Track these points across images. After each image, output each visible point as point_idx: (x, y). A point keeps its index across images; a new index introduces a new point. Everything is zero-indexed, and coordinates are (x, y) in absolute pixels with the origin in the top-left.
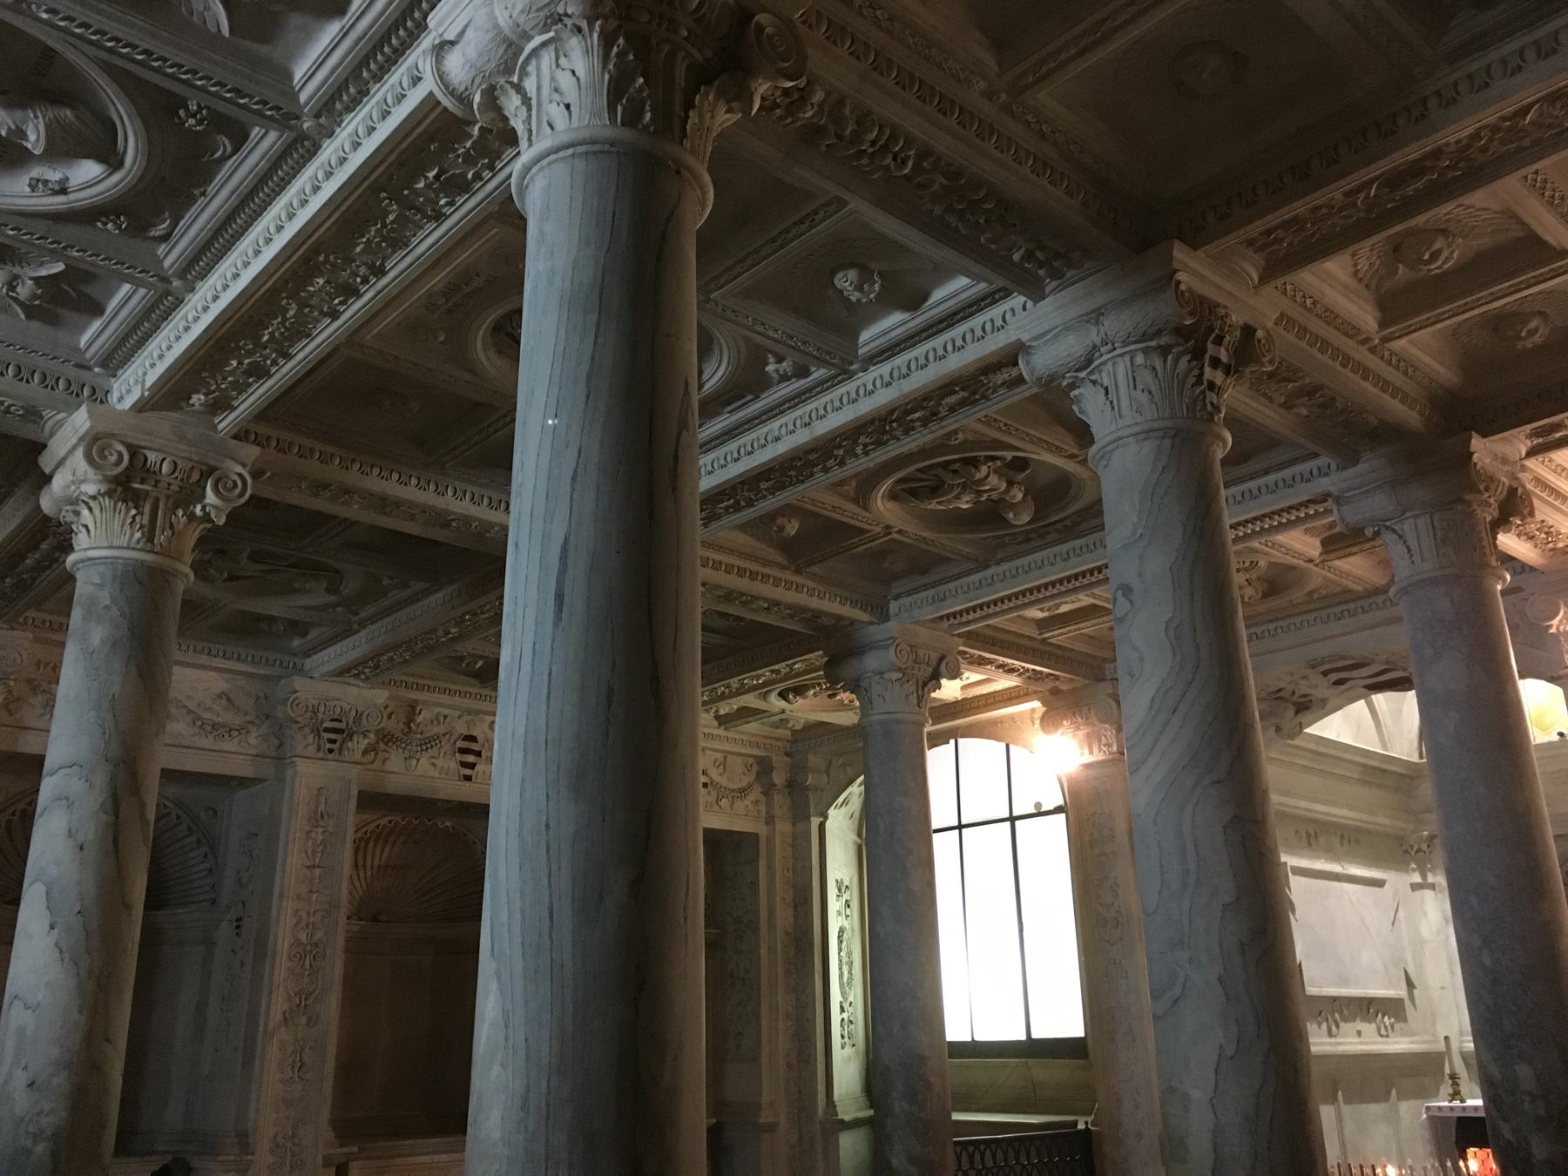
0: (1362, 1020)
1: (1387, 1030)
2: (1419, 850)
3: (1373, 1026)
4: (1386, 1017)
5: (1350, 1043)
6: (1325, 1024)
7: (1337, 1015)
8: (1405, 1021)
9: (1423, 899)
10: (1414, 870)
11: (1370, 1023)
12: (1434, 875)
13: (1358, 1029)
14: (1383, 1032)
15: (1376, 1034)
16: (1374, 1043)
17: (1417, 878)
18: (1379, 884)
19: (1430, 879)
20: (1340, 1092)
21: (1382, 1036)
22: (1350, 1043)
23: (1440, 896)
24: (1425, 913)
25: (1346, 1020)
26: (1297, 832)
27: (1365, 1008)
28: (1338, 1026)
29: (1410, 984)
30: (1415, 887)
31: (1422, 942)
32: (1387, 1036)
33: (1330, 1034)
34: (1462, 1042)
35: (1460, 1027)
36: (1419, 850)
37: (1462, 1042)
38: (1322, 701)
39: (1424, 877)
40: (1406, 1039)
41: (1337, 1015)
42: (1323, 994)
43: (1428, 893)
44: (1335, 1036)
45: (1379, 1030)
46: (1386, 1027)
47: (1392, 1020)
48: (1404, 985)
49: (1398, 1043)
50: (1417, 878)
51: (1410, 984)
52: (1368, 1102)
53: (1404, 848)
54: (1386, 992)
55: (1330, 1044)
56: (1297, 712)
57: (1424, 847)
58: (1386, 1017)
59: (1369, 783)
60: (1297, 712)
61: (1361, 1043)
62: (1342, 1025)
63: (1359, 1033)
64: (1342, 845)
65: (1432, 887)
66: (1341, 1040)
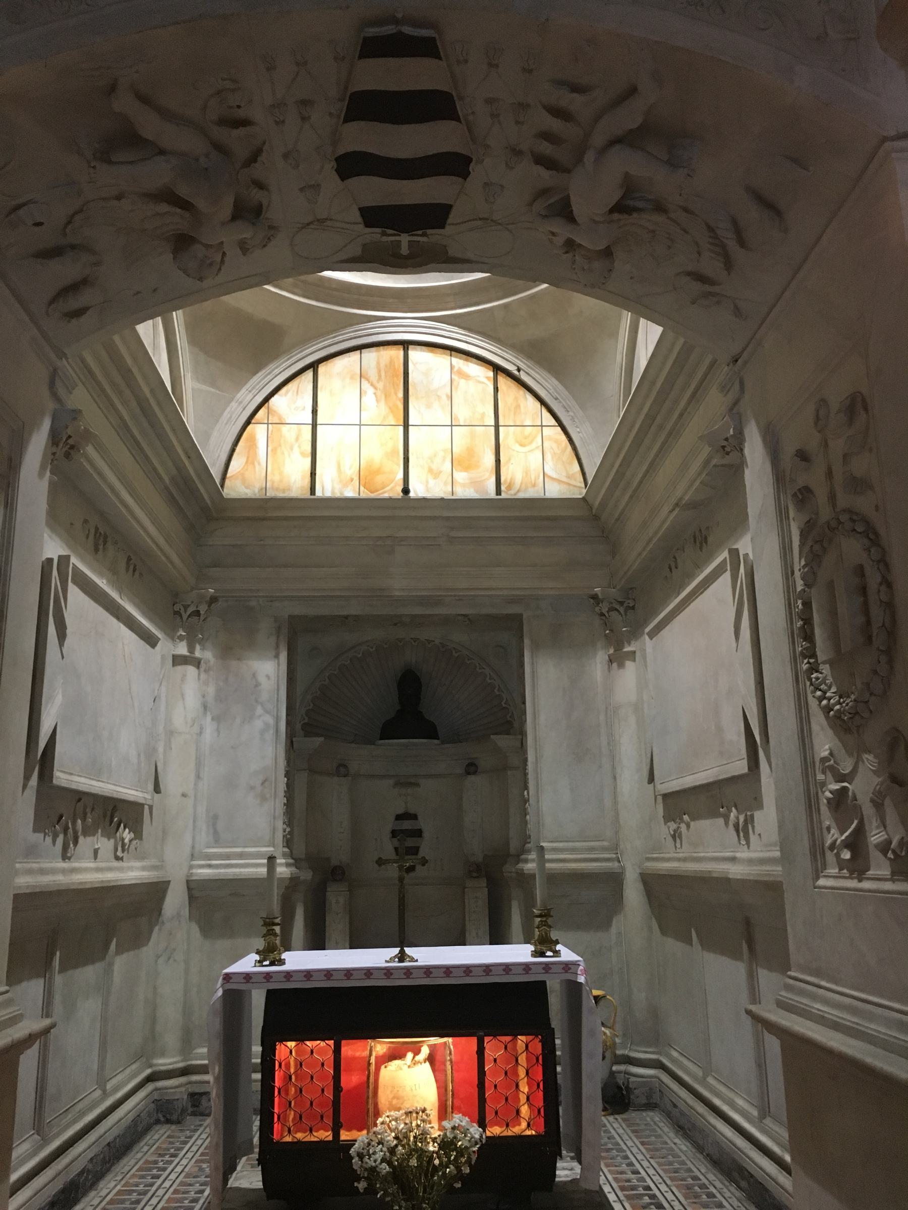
0: (102, 836)
1: (123, 851)
2: (197, 613)
3: (112, 841)
4: (127, 830)
5: (86, 870)
6: (60, 840)
7: (79, 821)
8: (141, 838)
9: (184, 676)
10: (181, 638)
11: (109, 839)
12: (203, 649)
13: (97, 847)
14: (119, 854)
15: (113, 856)
16: (110, 869)
17: (182, 649)
18: (151, 641)
19: (198, 654)
20: (58, 953)
21: (117, 858)
22: (86, 870)
23: (203, 676)
24: (183, 695)
25: (87, 832)
26: (86, 521)
27: (108, 819)
28: (76, 842)
29: (157, 789)
30: (178, 660)
31: (171, 733)
32: (122, 859)
33: (65, 857)
34: (191, 867)
35: (193, 847)
36: (197, 613)
37: (191, 867)
38: (271, 227)
39: (191, 649)
40: (138, 864)
41: (79, 821)
42: (74, 786)
43: (191, 670)
44: (69, 858)
45: (116, 850)
46: (123, 845)
47: (132, 835)
48: (151, 787)
49: (131, 869)
50: (182, 649)
51: (157, 789)
52: (85, 964)
53: (176, 608)
54: (140, 794)
55: (64, 871)
56: (234, 218)
57: (203, 609)
58: (127, 830)
59: (171, 500)
60: (234, 218)
61: (98, 870)
62: (81, 839)
63: (96, 852)
64: (127, 570)
65: (197, 663)
66: (76, 865)
